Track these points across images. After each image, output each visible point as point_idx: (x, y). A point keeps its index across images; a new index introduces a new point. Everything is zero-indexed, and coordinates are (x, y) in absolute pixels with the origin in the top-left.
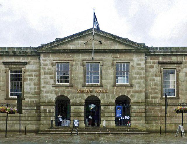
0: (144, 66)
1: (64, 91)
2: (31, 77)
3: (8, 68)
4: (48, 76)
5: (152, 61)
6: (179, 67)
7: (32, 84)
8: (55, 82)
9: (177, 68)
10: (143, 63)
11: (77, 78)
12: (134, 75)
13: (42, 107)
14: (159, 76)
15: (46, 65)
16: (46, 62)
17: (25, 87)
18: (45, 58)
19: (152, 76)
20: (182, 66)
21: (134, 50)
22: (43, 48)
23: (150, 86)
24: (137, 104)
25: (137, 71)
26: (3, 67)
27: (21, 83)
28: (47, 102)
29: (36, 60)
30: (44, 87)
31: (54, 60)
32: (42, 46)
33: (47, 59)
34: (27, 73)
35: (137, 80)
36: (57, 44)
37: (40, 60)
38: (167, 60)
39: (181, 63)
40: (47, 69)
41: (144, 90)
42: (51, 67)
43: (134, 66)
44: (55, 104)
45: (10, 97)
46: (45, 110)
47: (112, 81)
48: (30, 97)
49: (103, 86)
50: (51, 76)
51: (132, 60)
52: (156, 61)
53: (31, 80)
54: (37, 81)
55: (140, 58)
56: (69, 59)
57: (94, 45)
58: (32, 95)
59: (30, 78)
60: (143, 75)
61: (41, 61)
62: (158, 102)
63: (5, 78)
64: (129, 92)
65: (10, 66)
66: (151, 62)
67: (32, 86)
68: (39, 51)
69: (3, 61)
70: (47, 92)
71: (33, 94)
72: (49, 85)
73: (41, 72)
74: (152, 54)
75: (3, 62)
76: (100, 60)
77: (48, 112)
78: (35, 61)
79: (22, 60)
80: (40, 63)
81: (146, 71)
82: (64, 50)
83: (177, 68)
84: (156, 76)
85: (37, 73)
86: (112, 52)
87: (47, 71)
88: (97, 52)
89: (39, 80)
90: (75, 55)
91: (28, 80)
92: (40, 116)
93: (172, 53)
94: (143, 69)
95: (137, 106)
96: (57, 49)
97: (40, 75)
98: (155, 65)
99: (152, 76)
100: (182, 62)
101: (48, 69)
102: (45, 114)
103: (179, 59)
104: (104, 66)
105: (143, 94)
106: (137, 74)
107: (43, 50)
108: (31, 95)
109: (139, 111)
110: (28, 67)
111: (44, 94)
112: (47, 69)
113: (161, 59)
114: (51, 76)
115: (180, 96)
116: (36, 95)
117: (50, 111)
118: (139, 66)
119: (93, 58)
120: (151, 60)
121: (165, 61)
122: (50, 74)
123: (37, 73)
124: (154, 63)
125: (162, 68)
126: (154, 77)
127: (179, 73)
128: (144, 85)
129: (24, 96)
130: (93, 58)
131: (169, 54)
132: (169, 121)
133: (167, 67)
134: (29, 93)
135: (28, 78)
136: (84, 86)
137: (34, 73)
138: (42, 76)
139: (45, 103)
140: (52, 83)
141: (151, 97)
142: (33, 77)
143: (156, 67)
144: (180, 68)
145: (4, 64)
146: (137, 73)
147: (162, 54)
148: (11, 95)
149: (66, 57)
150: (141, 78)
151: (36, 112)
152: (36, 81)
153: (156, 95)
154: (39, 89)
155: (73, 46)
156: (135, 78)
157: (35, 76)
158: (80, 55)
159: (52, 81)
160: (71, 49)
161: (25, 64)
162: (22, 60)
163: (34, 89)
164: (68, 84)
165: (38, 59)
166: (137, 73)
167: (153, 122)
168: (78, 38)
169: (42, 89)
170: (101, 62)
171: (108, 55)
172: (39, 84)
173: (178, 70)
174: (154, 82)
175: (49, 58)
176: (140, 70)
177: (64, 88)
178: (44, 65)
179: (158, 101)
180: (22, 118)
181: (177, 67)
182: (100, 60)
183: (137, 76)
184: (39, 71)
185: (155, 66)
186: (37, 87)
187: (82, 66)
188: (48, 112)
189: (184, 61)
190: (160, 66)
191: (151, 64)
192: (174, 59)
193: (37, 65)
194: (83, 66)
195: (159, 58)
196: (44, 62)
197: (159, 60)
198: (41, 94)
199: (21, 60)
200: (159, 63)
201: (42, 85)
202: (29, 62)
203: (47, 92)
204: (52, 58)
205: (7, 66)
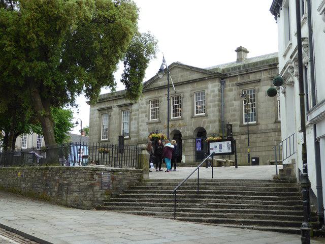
5: (231, 84)
15: (143, 104)
19: (231, 101)
20: (261, 83)
38: (246, 79)
39: (259, 81)
42: (146, 105)
56: (159, 95)
57: (177, 77)
62: (237, 131)
64: (204, 122)
69: (117, 104)
76: (181, 93)
84: (235, 100)
86: (188, 82)
88: (177, 85)
98: (234, 88)
106: (212, 102)
113: (239, 80)
120: (230, 82)
124: (233, 85)
126: (234, 102)
130: (176, 92)
143: (235, 90)
146: (212, 101)
150: (214, 106)
166: (212, 101)
171: (187, 85)
174: (233, 107)
176: (215, 97)
181: (256, 86)
192: (252, 77)
195: (237, 78)
204: (147, 97)
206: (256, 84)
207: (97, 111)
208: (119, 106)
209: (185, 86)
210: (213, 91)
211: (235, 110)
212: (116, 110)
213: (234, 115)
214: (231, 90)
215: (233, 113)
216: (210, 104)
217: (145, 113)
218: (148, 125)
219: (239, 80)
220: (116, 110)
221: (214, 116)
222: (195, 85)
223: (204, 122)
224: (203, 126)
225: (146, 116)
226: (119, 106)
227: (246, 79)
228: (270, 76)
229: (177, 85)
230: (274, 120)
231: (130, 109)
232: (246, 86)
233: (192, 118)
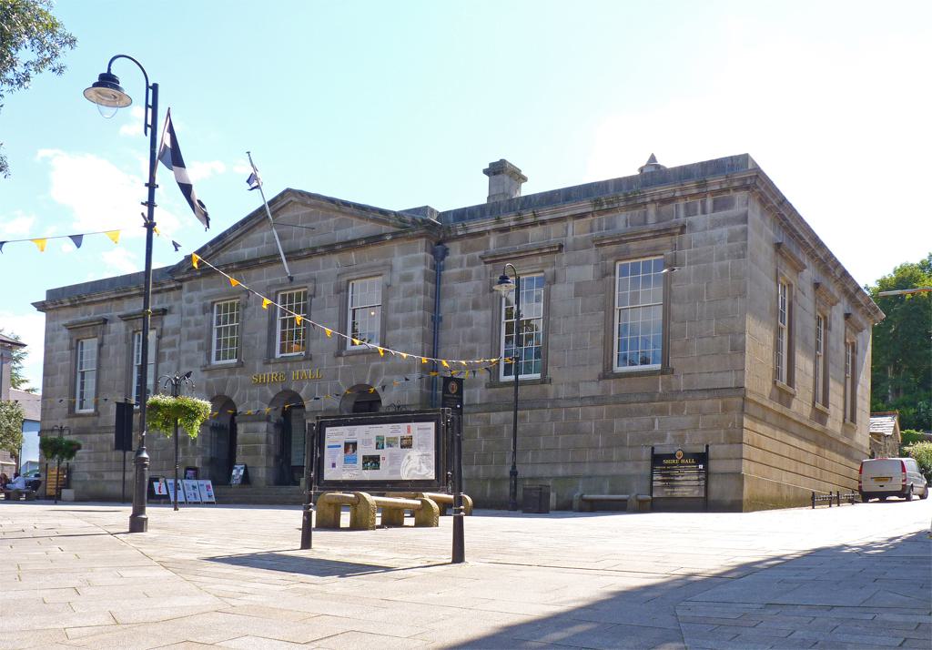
2: (172, 350)
11: (253, 342)
12: (393, 316)
19: (465, 308)
20: (564, 258)
35: (400, 331)
49: (311, 359)
60: (416, 313)
66: (462, 261)
84: (476, 306)
104: (318, 298)
118: (406, 284)
126: (472, 312)
130: (291, 279)
145: (125, 320)
150: (409, 323)
156: (396, 326)
160: (246, 258)
170: (310, 285)
176: (411, 295)
189: (570, 239)
191: (461, 266)
207: (65, 332)
212: (118, 328)
217: (199, 338)
218: (206, 374)
220: (118, 328)
223: (376, 372)
233: (339, 355)
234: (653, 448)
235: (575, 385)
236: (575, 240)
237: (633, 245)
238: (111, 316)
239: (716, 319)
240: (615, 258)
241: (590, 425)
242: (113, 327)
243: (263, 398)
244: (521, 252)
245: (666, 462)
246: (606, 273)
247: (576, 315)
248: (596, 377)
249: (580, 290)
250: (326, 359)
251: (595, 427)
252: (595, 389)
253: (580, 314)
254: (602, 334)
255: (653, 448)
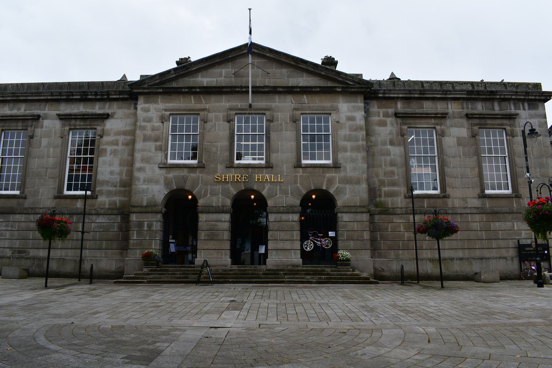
0: (362, 123)
1: (185, 179)
2: (115, 147)
3: (67, 128)
4: (152, 145)
5: (381, 111)
6: (441, 124)
7: (116, 162)
8: (166, 158)
9: (438, 127)
10: (360, 115)
11: (214, 149)
12: (342, 143)
13: (134, 218)
14: (399, 145)
15: (149, 120)
16: (149, 114)
17: (99, 169)
18: (147, 105)
19: (384, 143)
20: (448, 122)
21: (339, 87)
22: (145, 84)
23: (381, 166)
24: (351, 209)
25: (348, 133)
26: (58, 124)
27: (92, 160)
28: (145, 204)
29: (129, 109)
30: (140, 169)
31: (166, 110)
32: (145, 79)
33: (152, 107)
34: (105, 139)
35: (349, 154)
36: (174, 76)
37: (136, 108)
39: (444, 116)
40: (149, 129)
41: (365, 176)
42: (158, 124)
43: (341, 121)
44: (164, 210)
45: (66, 193)
46: (140, 225)
47: (291, 156)
48: (109, 193)
49: (272, 167)
50: (158, 143)
51: (336, 109)
52: (391, 111)
53: (114, 152)
54: (126, 155)
55: (353, 104)
56: (198, 106)
58: (114, 189)
59: (111, 150)
61: (139, 111)
63: (58, 150)
65: (73, 122)
66: (379, 113)
67: (116, 168)
68: (135, 91)
69: (58, 112)
70: (148, 181)
71: (116, 186)
72: (152, 165)
73: (136, 135)
74: (380, 95)
75: (58, 115)
76: (265, 110)
77: (146, 228)
78: (126, 111)
79: (100, 109)
80: (135, 114)
81: (368, 134)
82: (188, 88)
83: (438, 127)
84: (392, 143)
85: (129, 138)
86: (290, 91)
87: (149, 132)
88: (258, 91)
89: (132, 154)
90: (213, 98)
91: (108, 153)
92: (126, 238)
93: (424, 94)
94: (361, 129)
95: (352, 215)
96: (174, 85)
97: (133, 143)
98: (389, 120)
99: (384, 143)
100: (447, 114)
101: (153, 129)
102: (139, 233)
103: (440, 107)
104: (275, 123)
105: (364, 186)
106: (349, 141)
107: (144, 88)
108: (111, 189)
109: (356, 226)
110: (109, 124)
111: (140, 186)
112: (149, 129)
114: (158, 143)
115: (449, 191)
116: (123, 189)
117: (150, 226)
119: (250, 106)
120: (379, 108)
121: (408, 110)
122: (156, 140)
123: (129, 138)
124: (386, 115)
125: (405, 127)
126: (389, 147)
127: (443, 138)
128: (365, 166)
129: (97, 189)
130: (250, 106)
131: (416, 96)
132: (429, 251)
133: (415, 124)
134: (107, 183)
135: (109, 148)
136: (231, 166)
137: (121, 138)
138: (139, 145)
139: (142, 207)
140: (159, 162)
141: (385, 192)
142: (120, 147)
144: (443, 127)
145: (60, 119)
146: (348, 139)
147: (401, 96)
148: (69, 189)
149: (191, 103)
150: (356, 149)
151: (120, 229)
152: (126, 156)
153: (396, 189)
154: (130, 174)
155: (208, 79)
156: (345, 150)
157: (123, 144)
158: (224, 97)
159: (159, 157)
160: (205, 85)
161: (106, 117)
162: (100, 109)
163: (120, 173)
164: (195, 162)
165: (132, 107)
166: (348, 139)
167: (392, 254)
168: (219, 63)
169: (137, 174)
170: (267, 113)
171: (282, 97)
172: (131, 164)
173: (440, 132)
175: (155, 106)
176: (356, 130)
177: (185, 172)
178: (144, 120)
179: (401, 203)
180: (87, 244)
181: (437, 124)
182: (265, 110)
183: (349, 144)
184: (133, 133)
185: (388, 123)
186: (125, 169)
187: (226, 123)
188: (146, 228)
189: (450, 111)
190: (399, 121)
191: (379, 116)
192: (428, 107)
193: (130, 121)
194: (229, 122)
195: (396, 104)
196: (145, 114)
197: (396, 108)
198: (133, 187)
199: (97, 109)
200: (396, 115)
201: (138, 165)
202: (114, 114)
203: (148, 181)
205: (67, 123)
206: (438, 121)
208: (63, 118)
209: (277, 97)
210: (351, 118)
211: (392, 164)
213: (393, 173)
214: (383, 124)
215: (389, 169)
216: (345, 143)
218: (163, 171)
219: (400, 106)
221: (354, 169)
222: (305, 98)
223: (330, 181)
224: (327, 187)
225: (159, 149)
226: (63, 118)
227: (414, 108)
228: (465, 111)
229: (258, 91)
230: (478, 191)
231: (99, 128)
232: (418, 121)
234: (518, 241)
235: (464, 199)
236: (453, 112)
237: (489, 121)
238: (45, 114)
239: (540, 168)
240: (479, 126)
241: (476, 226)
242: (46, 123)
243: (225, 193)
244: (423, 114)
245: (527, 249)
246: (474, 136)
247: (460, 157)
248: (476, 195)
249: (460, 142)
250: (286, 168)
251: (480, 226)
252: (476, 203)
253: (462, 156)
254: (477, 170)
255: (518, 241)
